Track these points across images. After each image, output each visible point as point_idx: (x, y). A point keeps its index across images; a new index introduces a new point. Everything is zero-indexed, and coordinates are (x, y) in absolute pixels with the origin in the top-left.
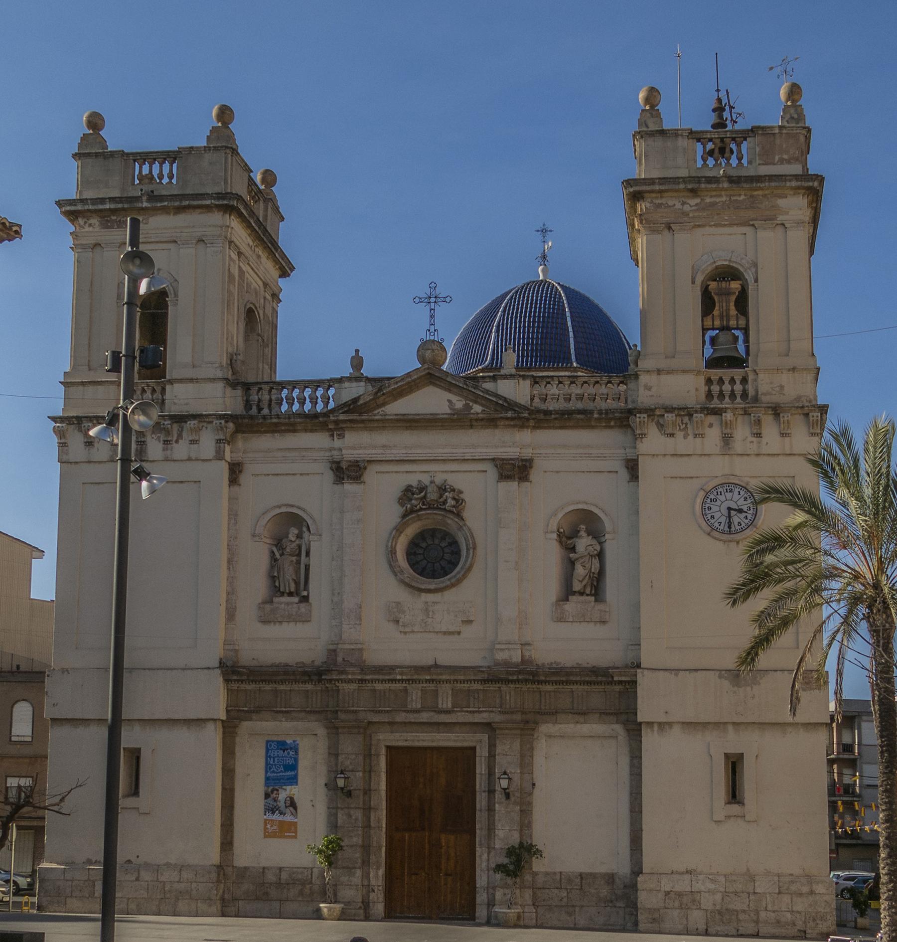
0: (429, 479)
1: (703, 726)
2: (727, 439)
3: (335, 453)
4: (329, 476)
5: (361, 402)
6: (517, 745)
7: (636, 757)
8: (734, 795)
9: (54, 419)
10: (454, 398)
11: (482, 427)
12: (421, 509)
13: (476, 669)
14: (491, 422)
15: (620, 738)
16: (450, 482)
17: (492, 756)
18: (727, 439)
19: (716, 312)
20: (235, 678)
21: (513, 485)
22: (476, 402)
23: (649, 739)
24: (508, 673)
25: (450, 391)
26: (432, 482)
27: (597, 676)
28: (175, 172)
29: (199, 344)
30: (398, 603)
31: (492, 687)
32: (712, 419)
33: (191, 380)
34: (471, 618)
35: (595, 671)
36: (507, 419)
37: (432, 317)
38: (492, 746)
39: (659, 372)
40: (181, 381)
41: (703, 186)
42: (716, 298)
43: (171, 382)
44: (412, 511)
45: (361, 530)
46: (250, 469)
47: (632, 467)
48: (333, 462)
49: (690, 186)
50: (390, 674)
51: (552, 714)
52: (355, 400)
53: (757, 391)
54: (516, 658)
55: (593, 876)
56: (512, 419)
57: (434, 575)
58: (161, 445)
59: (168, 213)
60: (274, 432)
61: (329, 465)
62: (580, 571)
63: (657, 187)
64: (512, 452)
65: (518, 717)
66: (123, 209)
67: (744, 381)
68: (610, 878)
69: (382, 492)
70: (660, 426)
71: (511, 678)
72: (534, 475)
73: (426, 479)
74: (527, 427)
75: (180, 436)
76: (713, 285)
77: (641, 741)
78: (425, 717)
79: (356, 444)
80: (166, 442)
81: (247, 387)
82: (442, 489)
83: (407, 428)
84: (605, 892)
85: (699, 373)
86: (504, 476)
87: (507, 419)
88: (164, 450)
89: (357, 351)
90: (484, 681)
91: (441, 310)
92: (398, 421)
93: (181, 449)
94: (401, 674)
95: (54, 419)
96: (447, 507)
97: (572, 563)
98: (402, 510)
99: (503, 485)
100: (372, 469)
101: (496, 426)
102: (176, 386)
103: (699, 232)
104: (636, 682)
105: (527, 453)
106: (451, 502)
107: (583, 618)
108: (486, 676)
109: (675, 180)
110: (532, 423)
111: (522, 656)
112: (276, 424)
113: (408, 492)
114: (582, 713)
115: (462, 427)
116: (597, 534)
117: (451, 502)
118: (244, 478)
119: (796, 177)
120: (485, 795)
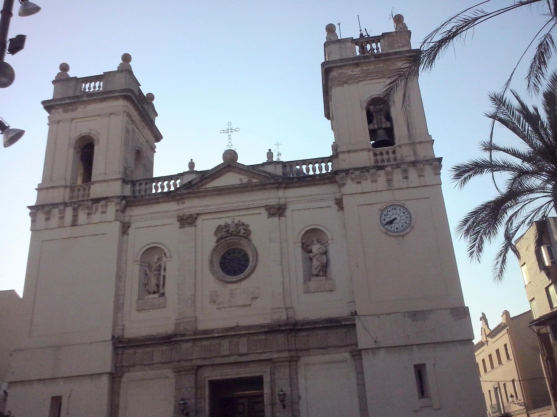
0: (231, 221)
3: (181, 212)
4: (178, 224)
5: (193, 183)
6: (287, 371)
7: (360, 372)
8: (422, 392)
9: (30, 207)
10: (242, 177)
11: (258, 190)
12: (227, 237)
13: (262, 326)
14: (262, 187)
15: (349, 362)
16: (242, 221)
17: (273, 381)
19: (375, 121)
20: (120, 345)
21: (276, 219)
22: (254, 178)
23: (367, 359)
24: (280, 326)
25: (240, 173)
27: (332, 324)
28: (101, 85)
29: (108, 162)
30: (215, 291)
31: (270, 337)
32: (380, 172)
33: (104, 181)
34: (257, 296)
35: (330, 320)
36: (271, 184)
37: (230, 139)
38: (272, 374)
39: (349, 152)
40: (99, 182)
41: (362, 61)
42: (374, 114)
43: (94, 183)
44: (222, 238)
45: (190, 252)
46: (133, 226)
47: (339, 203)
48: (178, 217)
49: (355, 62)
50: (211, 333)
52: (190, 182)
53: (402, 157)
54: (284, 317)
56: (274, 184)
57: (235, 274)
58: (86, 216)
59: (97, 102)
60: (147, 204)
61: (176, 219)
62: (315, 263)
63: (339, 64)
64: (273, 201)
65: (286, 354)
66: (74, 102)
67: (394, 152)
69: (207, 229)
70: (352, 179)
71: (281, 329)
72: (288, 212)
73: (229, 221)
74: (281, 188)
75: (96, 210)
76: (372, 108)
77: (362, 363)
78: (232, 359)
79: (191, 206)
80: (89, 214)
81: (133, 183)
82: (237, 225)
83: (218, 195)
85: (369, 150)
86: (271, 215)
87: (271, 184)
88: (88, 218)
89: (192, 160)
90: (266, 333)
91: (234, 135)
92: (213, 191)
93: (96, 217)
94: (217, 333)
95: (30, 207)
96: (241, 234)
97: (311, 259)
98: (215, 239)
99: (271, 219)
100: (201, 218)
101: (265, 189)
102: (96, 185)
103: (361, 84)
104: (355, 325)
105: (282, 202)
106: (242, 231)
108: (266, 329)
109: (348, 60)
110: (284, 186)
111: (287, 315)
112: (149, 200)
113: (219, 228)
115: (248, 191)
116: (323, 242)
117: (242, 231)
118: (131, 231)
119: (408, 51)
120: (270, 407)
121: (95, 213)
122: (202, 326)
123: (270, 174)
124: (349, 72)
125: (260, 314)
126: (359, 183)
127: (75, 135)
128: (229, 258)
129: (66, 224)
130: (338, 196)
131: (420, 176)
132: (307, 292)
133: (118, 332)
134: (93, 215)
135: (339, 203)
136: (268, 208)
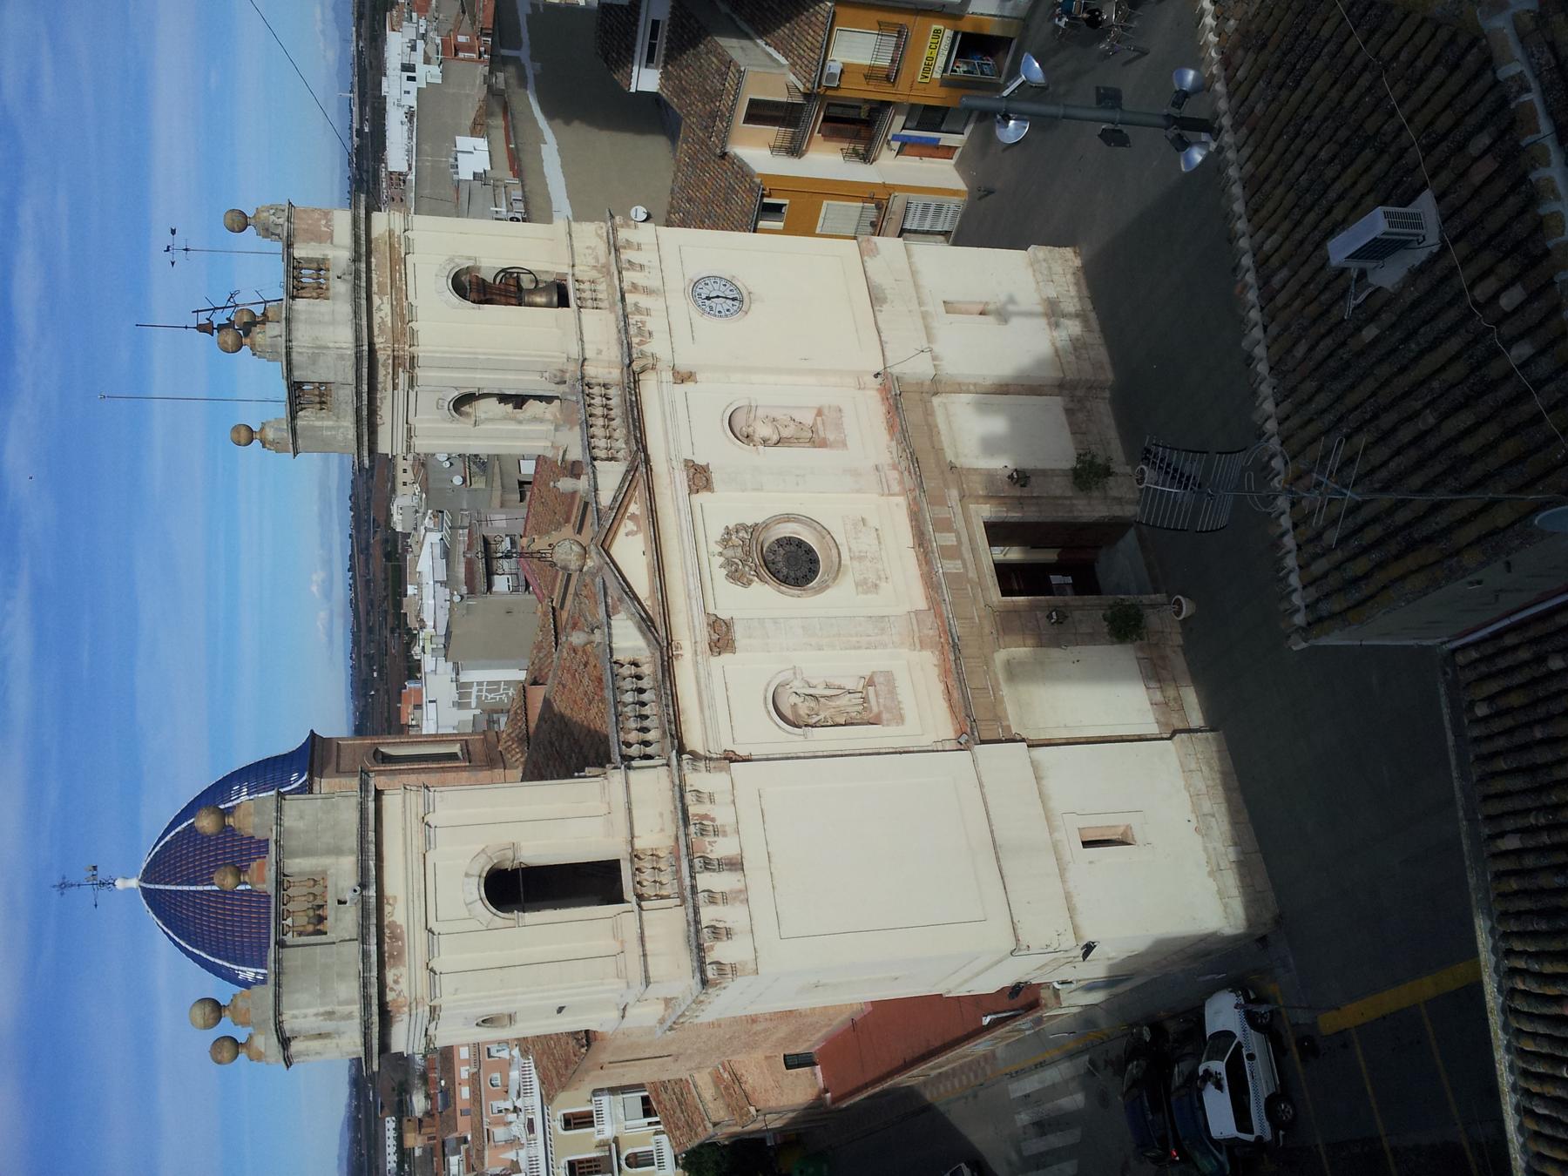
1: (928, 329)
2: (647, 291)
4: (726, 657)
10: (622, 531)
18: (647, 291)
26: (721, 554)
30: (857, 585)
47: (683, 377)
51: (938, 451)
55: (1070, 424)
58: (720, 840)
61: (713, 659)
64: (681, 478)
68: (1069, 412)
70: (641, 343)
72: (701, 461)
75: (706, 817)
78: (968, 555)
79: (688, 632)
80: (716, 833)
82: (725, 542)
84: (1081, 416)
86: (708, 486)
88: (725, 834)
93: (721, 814)
105: (679, 467)
107: (839, 426)
113: (735, 576)
114: (931, 430)
121: (713, 820)
122: (922, 604)
123: (628, 471)
124: (383, 309)
125: (891, 517)
126: (650, 334)
127: (484, 912)
128: (785, 571)
129: (740, 886)
130: (668, 376)
131: (639, 247)
132: (844, 444)
133: (953, 745)
134: (718, 823)
135: (683, 377)
136: (694, 489)
